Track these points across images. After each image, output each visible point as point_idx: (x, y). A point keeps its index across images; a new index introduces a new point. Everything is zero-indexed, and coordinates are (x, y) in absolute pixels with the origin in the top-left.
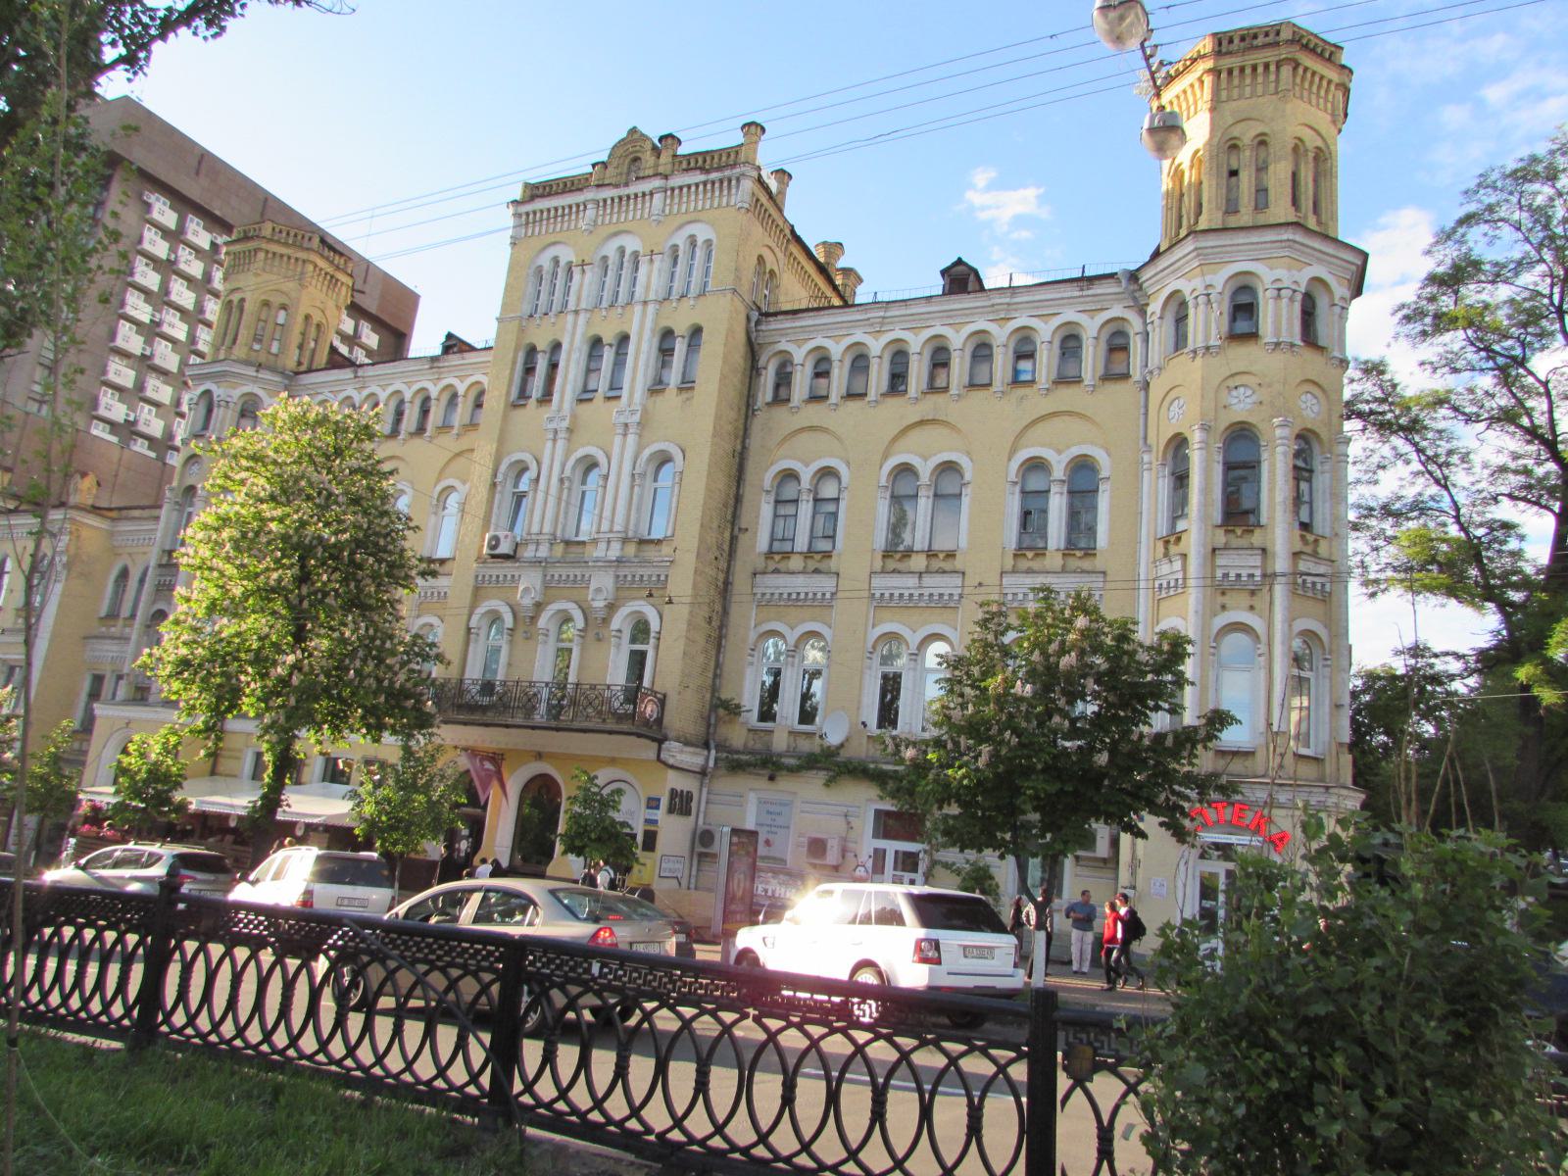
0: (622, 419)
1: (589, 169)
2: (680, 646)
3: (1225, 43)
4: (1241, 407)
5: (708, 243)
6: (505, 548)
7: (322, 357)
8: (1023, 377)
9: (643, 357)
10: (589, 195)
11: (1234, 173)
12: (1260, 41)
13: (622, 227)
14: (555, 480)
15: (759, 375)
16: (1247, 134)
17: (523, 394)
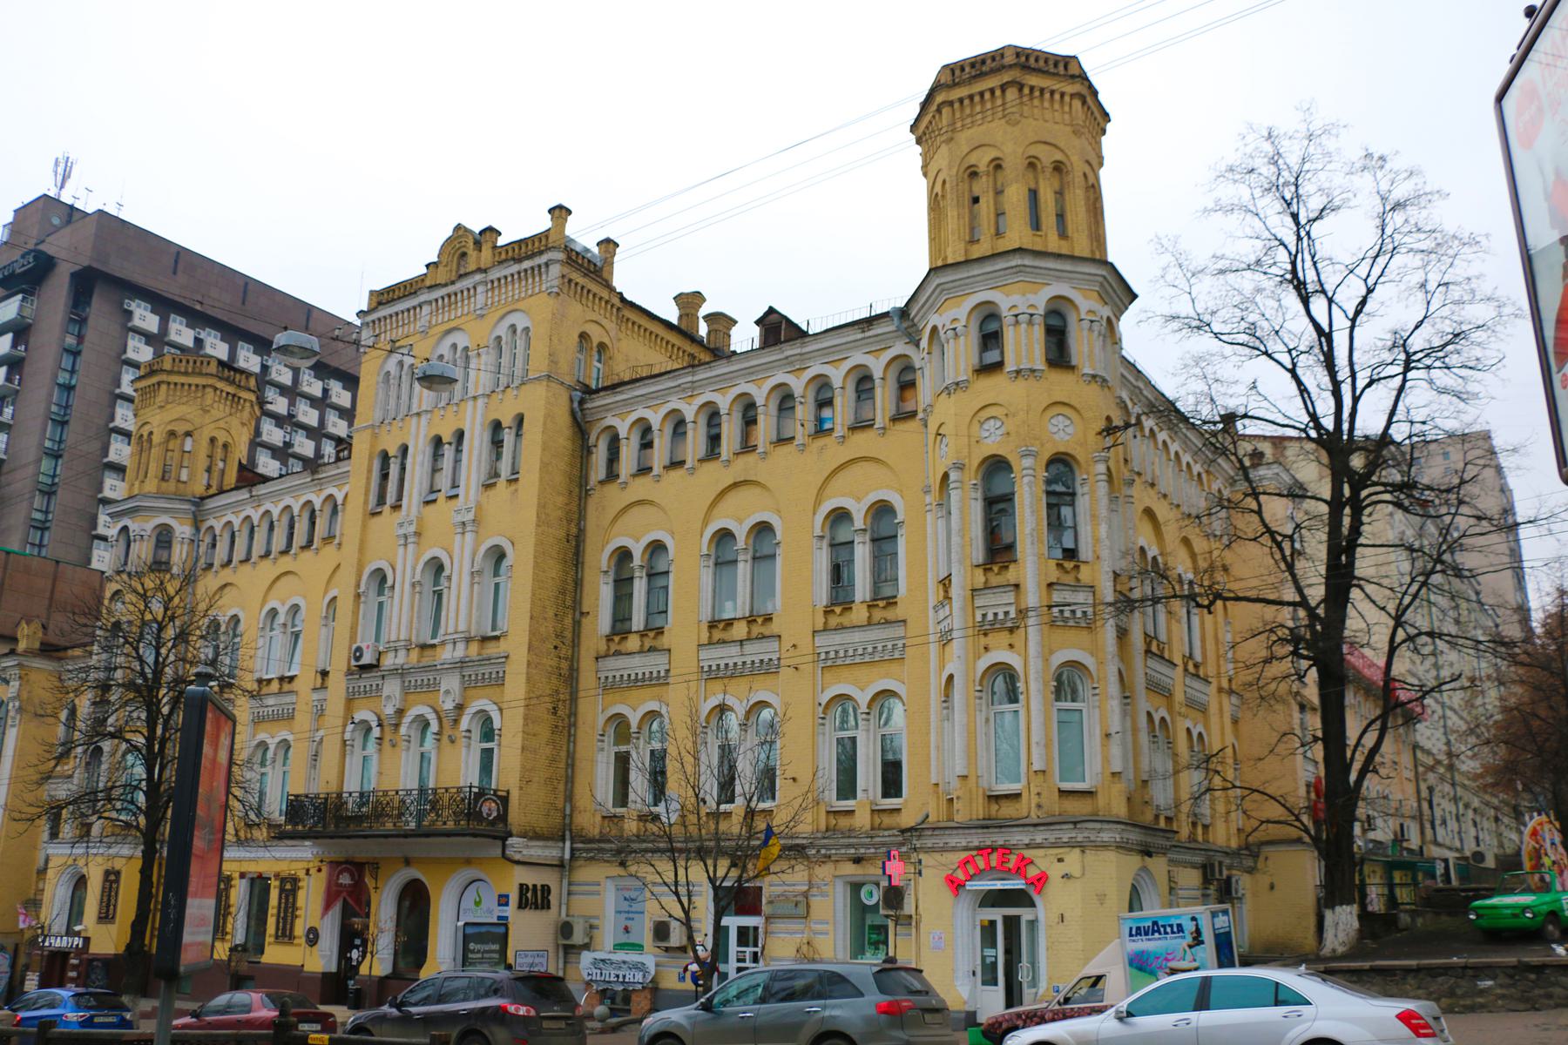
0: (460, 519)
1: (424, 270)
2: (518, 741)
3: (957, 72)
4: (992, 442)
5: (527, 329)
6: (367, 659)
7: (231, 477)
8: (827, 426)
9: (476, 453)
10: (423, 298)
11: (976, 200)
12: (989, 64)
13: (453, 324)
14: (407, 586)
15: (589, 452)
16: (982, 160)
17: (381, 500)
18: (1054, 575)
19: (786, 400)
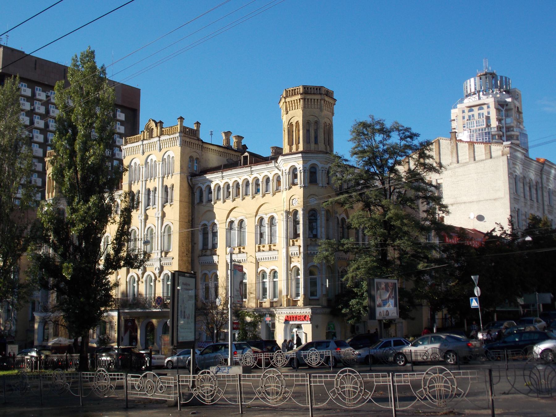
15: (194, 195)
18: (309, 242)
19: (247, 184)
